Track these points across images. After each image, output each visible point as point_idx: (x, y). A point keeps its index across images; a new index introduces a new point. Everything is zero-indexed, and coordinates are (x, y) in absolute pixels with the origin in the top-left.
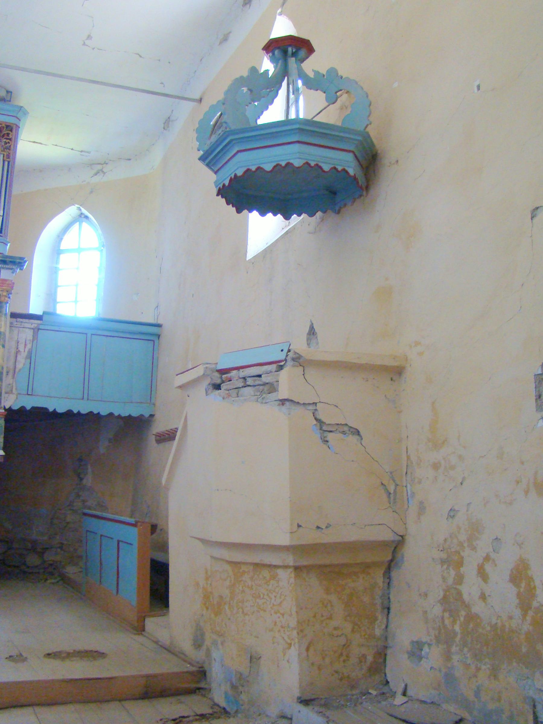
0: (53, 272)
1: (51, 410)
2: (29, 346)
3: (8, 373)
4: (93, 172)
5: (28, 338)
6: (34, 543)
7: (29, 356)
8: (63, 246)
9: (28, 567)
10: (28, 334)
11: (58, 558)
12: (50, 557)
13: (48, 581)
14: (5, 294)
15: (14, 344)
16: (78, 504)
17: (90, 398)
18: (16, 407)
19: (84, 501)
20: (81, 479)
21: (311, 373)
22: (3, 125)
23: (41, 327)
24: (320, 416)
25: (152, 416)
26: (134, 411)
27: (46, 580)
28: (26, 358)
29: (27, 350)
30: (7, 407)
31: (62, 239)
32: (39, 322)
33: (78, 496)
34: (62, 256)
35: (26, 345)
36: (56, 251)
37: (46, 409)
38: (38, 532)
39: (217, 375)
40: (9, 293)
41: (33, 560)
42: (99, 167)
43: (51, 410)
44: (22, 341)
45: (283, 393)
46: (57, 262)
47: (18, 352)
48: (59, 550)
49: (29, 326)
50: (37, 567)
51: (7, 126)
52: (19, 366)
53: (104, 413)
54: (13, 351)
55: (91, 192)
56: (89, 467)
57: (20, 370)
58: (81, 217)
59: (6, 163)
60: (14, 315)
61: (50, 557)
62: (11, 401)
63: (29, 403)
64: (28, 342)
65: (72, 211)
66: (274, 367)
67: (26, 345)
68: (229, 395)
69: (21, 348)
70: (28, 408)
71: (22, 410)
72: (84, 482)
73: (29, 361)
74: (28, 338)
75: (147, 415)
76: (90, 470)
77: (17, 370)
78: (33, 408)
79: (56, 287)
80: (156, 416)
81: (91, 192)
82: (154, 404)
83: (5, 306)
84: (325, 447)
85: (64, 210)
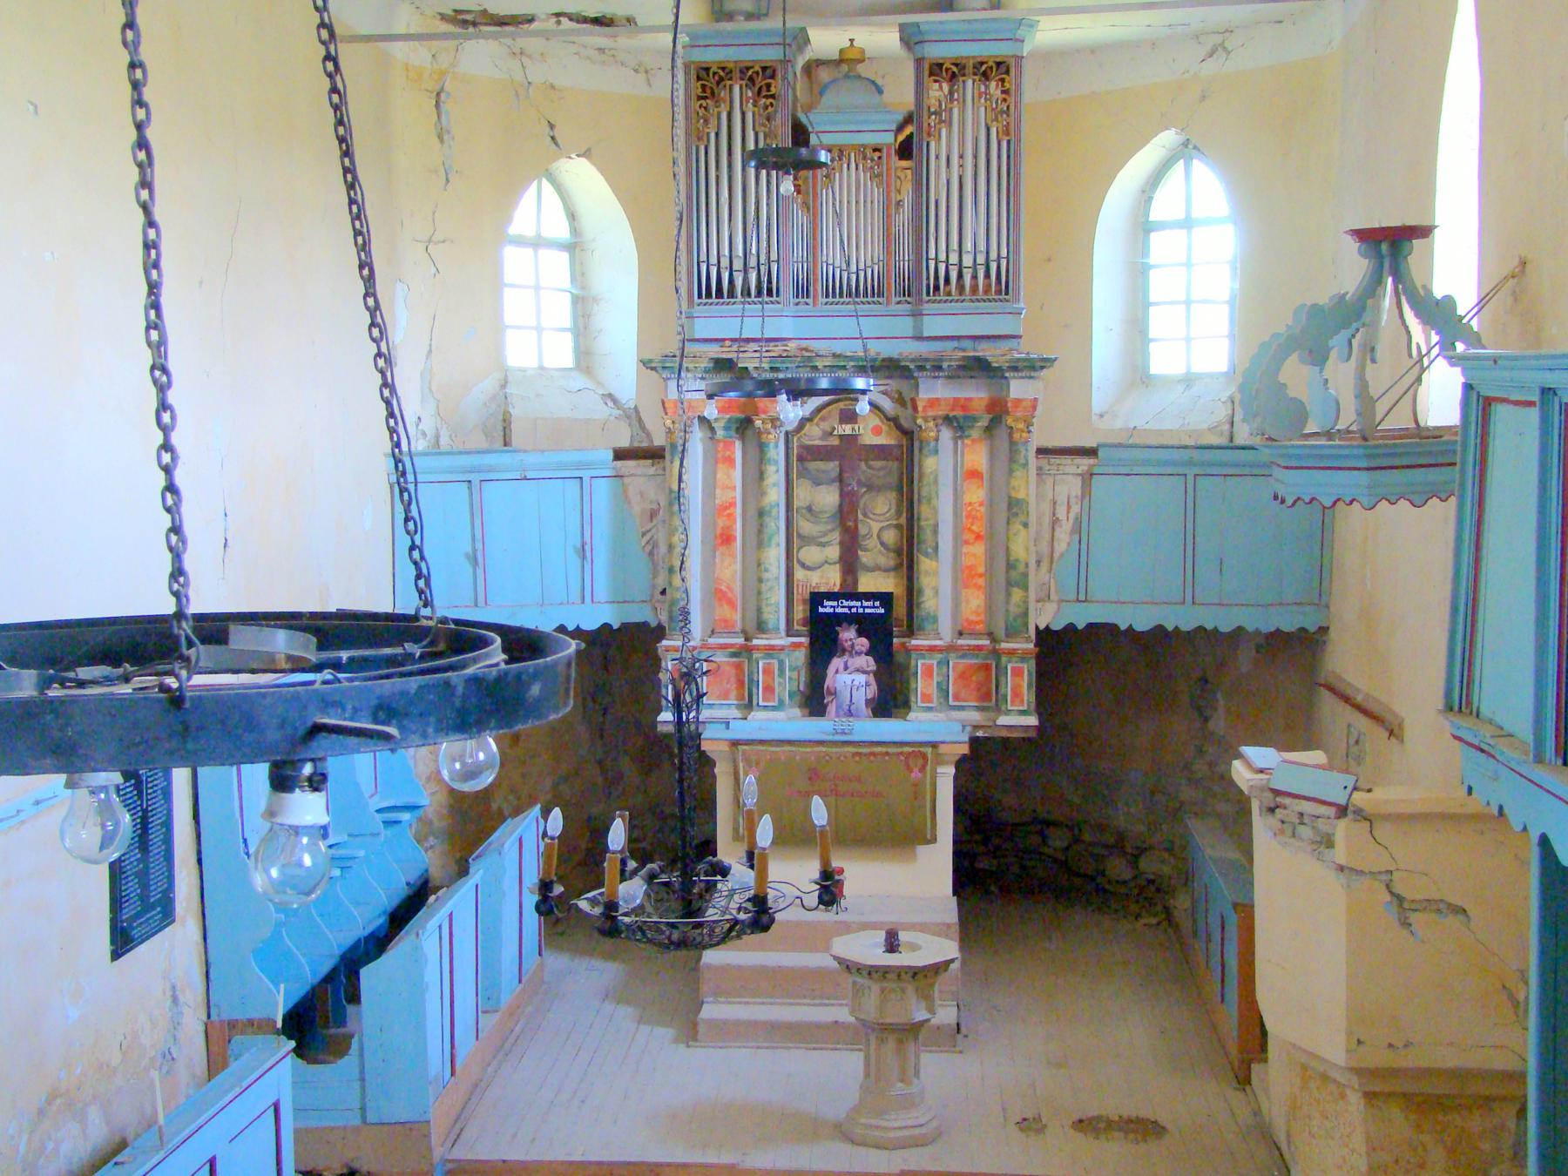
0: (1138, 274)
1: (1123, 627)
2: (1076, 508)
3: (1038, 562)
4: (1208, 48)
5: (1073, 494)
6: (1121, 838)
7: (1077, 528)
8: (1156, 214)
9: (1109, 882)
10: (1073, 486)
11: (1166, 870)
12: (1148, 865)
13: (1143, 921)
14: (1021, 426)
15: (1046, 507)
16: (1200, 768)
17: (1197, 600)
18: (1057, 626)
19: (1211, 764)
20: (1206, 720)
21: (1382, 831)
22: (991, 63)
23: (1096, 470)
24: (1398, 888)
25: (1324, 630)
26: (1288, 623)
27: (1137, 917)
28: (1072, 532)
29: (1072, 515)
30: (1042, 627)
31: (1150, 199)
32: (1092, 461)
33: (1200, 752)
34: (1152, 235)
35: (1069, 507)
36: (1142, 227)
37: (1115, 626)
38: (1128, 815)
39: (1269, 795)
40: (1029, 424)
41: (1118, 868)
42: (1217, 39)
43: (1123, 627)
44: (1062, 500)
45: (1340, 854)
46: (1145, 252)
47: (1055, 522)
48: (1166, 855)
49: (1073, 470)
50: (1125, 882)
51: (999, 64)
52: (1061, 547)
53: (1225, 628)
54: (1046, 521)
55: (1203, 98)
56: (1219, 696)
57: (1062, 555)
58: (1186, 150)
59: (1004, 144)
60: (1041, 451)
61: (1148, 865)
62: (1047, 616)
63: (1081, 617)
64: (1073, 501)
65: (1167, 139)
66: (1331, 811)
67: (1069, 507)
68: (1282, 832)
69: (1061, 513)
70: (1081, 626)
71: (1071, 628)
72: (1211, 725)
73: (1076, 537)
74: (1073, 494)
75: (1312, 629)
76: (1222, 702)
77: (1056, 556)
78: (1090, 625)
79: (1146, 305)
80: (1332, 634)
81: (1203, 98)
82: (1327, 607)
83: (1022, 449)
84: (1405, 932)
85: (1148, 142)
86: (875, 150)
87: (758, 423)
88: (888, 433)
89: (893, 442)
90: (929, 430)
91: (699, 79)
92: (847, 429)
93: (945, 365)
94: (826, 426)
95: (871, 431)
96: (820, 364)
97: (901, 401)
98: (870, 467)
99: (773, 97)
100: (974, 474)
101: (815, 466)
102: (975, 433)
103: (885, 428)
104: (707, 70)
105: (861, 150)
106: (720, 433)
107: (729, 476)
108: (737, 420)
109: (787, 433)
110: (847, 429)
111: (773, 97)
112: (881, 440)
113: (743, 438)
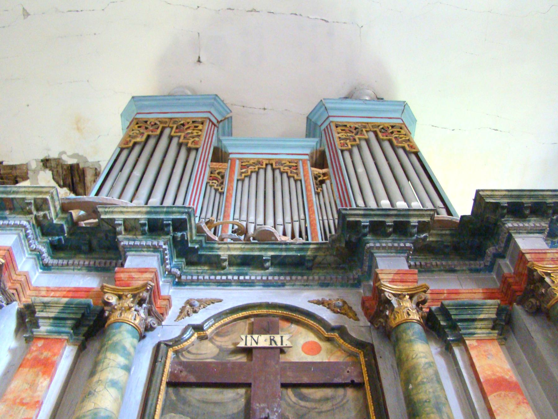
51: (392, 127)
86: (290, 162)
87: (113, 300)
88: (331, 353)
89: (341, 360)
90: (408, 311)
91: (137, 124)
92: (263, 341)
93: (414, 221)
94: (227, 343)
95: (298, 345)
96: (224, 254)
97: (342, 309)
98: (303, 398)
99: (201, 130)
100: (501, 384)
101: (196, 395)
102: (481, 331)
103: (323, 344)
104: (146, 122)
105: (279, 162)
106: (44, 328)
107: (33, 385)
108: (79, 306)
109: (158, 346)
110: (263, 341)
111: (201, 130)
112: (321, 357)
113: (82, 348)
